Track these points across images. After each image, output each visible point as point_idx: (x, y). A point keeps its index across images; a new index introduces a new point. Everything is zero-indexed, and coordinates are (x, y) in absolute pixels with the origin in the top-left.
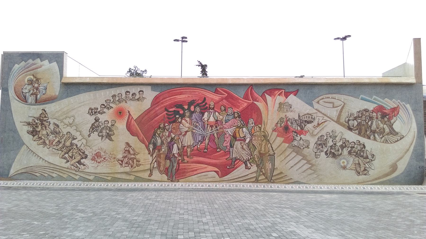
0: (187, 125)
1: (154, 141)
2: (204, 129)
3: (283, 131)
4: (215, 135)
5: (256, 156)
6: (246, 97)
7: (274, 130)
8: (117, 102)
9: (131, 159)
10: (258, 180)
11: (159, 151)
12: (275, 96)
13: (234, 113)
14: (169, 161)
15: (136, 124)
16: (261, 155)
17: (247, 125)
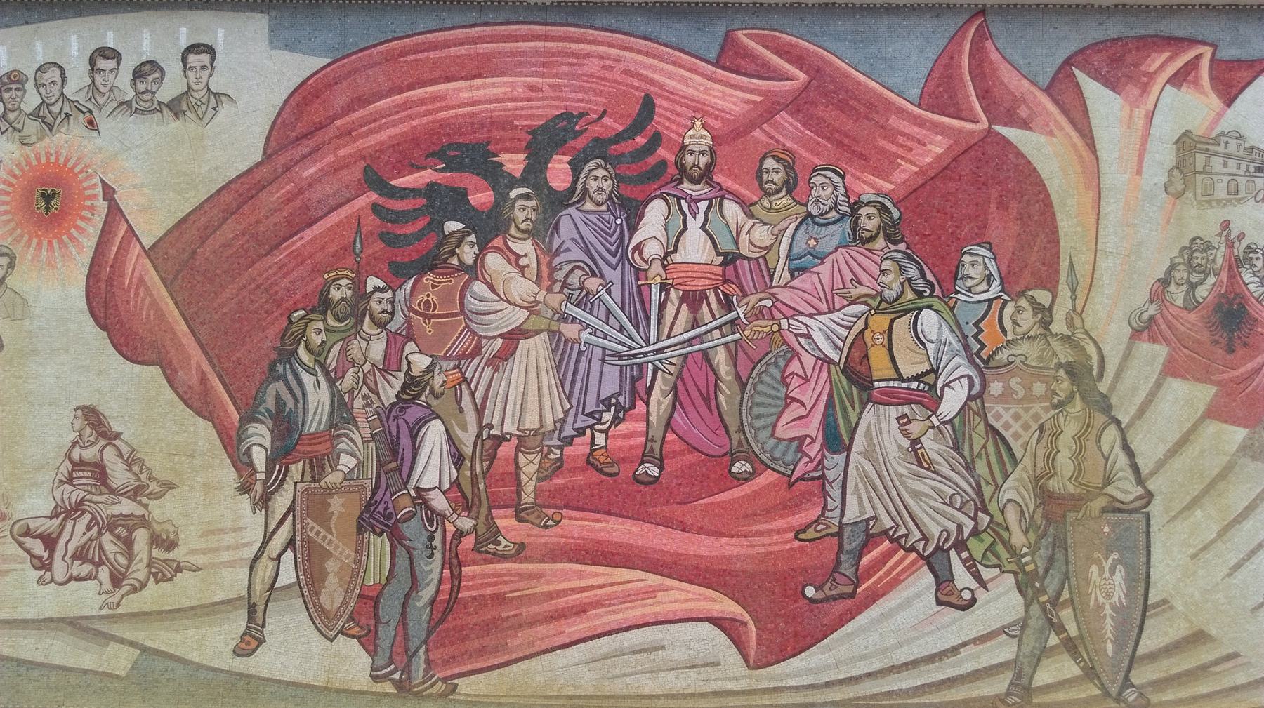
0: (522, 288)
1: (279, 402)
2: (640, 316)
3: (1205, 336)
4: (721, 359)
5: (1012, 516)
6: (941, 95)
7: (1145, 330)
8: (32, 127)
9: (111, 527)
10: (1028, 690)
11: (318, 467)
12: (1145, 89)
13: (855, 207)
14: (383, 543)
15: (153, 279)
16: (1053, 507)
17: (948, 294)
